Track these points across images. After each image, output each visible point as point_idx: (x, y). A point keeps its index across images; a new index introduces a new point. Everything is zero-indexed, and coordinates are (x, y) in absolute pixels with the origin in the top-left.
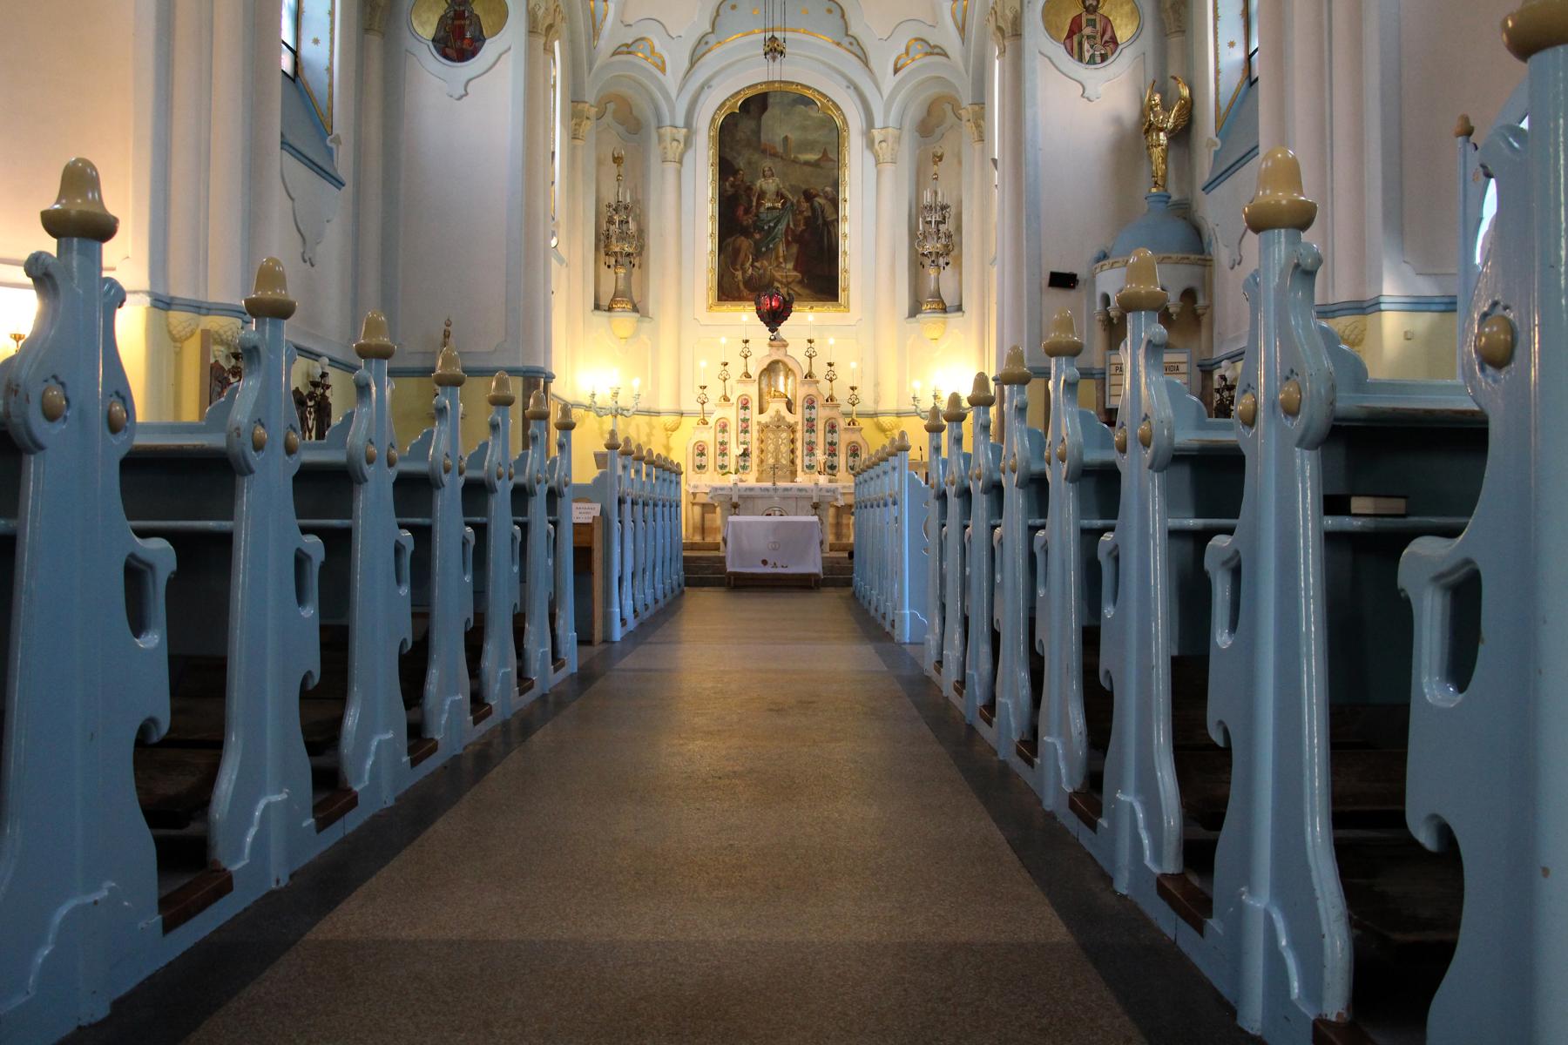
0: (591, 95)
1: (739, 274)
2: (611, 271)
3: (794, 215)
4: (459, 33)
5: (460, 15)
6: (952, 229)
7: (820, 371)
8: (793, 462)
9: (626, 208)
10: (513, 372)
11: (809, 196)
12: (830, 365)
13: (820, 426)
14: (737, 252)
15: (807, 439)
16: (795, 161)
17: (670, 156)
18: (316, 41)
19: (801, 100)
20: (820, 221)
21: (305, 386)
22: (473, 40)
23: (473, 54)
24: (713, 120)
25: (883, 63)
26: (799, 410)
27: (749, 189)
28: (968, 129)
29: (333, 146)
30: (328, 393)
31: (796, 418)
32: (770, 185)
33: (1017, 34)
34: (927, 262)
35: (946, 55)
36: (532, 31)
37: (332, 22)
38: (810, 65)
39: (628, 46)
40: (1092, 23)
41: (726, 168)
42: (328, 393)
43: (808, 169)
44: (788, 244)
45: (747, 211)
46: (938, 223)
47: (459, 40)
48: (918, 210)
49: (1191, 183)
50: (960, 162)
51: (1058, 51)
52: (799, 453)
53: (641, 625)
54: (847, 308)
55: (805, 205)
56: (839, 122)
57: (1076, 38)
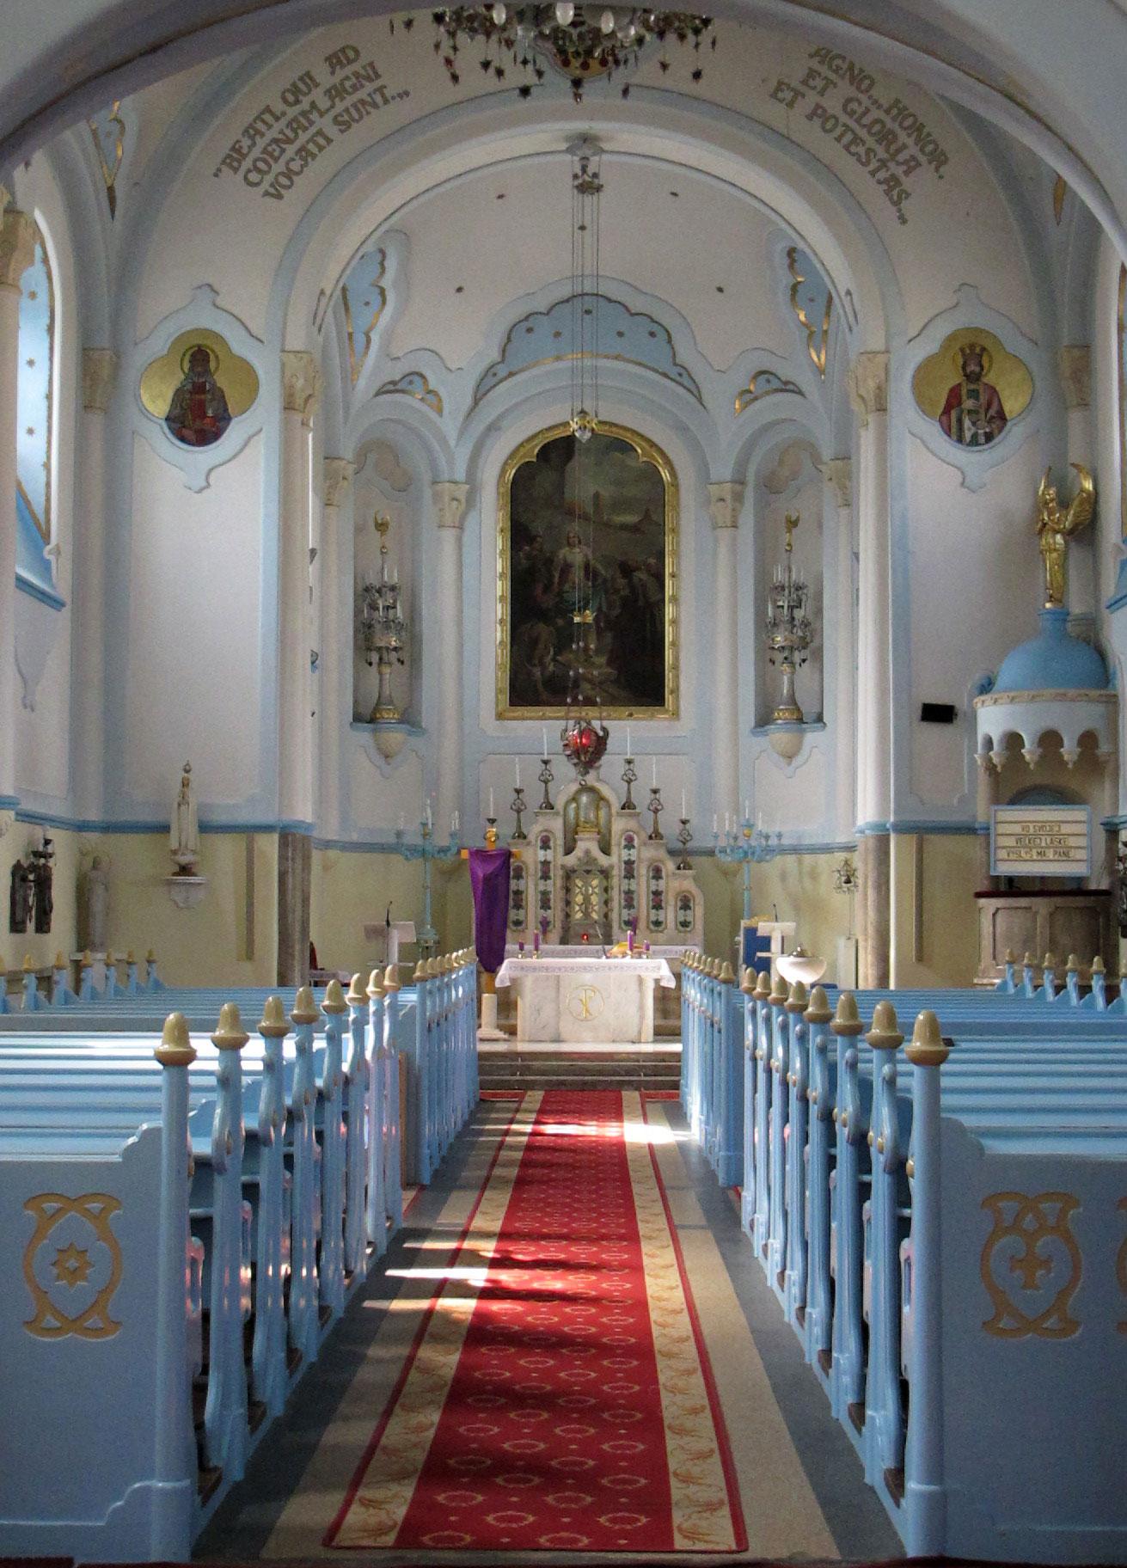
0: (348, 450)
1: (537, 672)
2: (374, 668)
3: (606, 592)
4: (199, 410)
5: (199, 389)
6: (811, 618)
7: (642, 798)
8: (606, 916)
9: (393, 588)
10: (267, 829)
11: (626, 570)
12: (655, 792)
13: (642, 871)
14: (535, 642)
15: (625, 887)
16: (607, 525)
17: (448, 520)
18: (30, 431)
19: (614, 444)
20: (640, 603)
21: (27, 856)
22: (216, 419)
23: (217, 436)
24: (503, 472)
25: (720, 393)
26: (614, 849)
27: (549, 562)
28: (829, 490)
29: (51, 558)
30: (51, 863)
31: (615, 860)
32: (577, 556)
33: (882, 409)
34: (779, 657)
35: (800, 393)
36: (288, 407)
37: (50, 408)
38: (625, 401)
39: (394, 383)
40: (974, 394)
41: (520, 535)
42: (51, 863)
43: (625, 535)
44: (600, 632)
45: (547, 588)
46: (791, 608)
47: (199, 417)
48: (767, 590)
49: (1097, 600)
50: (820, 526)
51: (932, 430)
52: (615, 904)
53: (443, 1159)
54: (676, 715)
55: (621, 582)
56: (666, 475)
57: (954, 414)
